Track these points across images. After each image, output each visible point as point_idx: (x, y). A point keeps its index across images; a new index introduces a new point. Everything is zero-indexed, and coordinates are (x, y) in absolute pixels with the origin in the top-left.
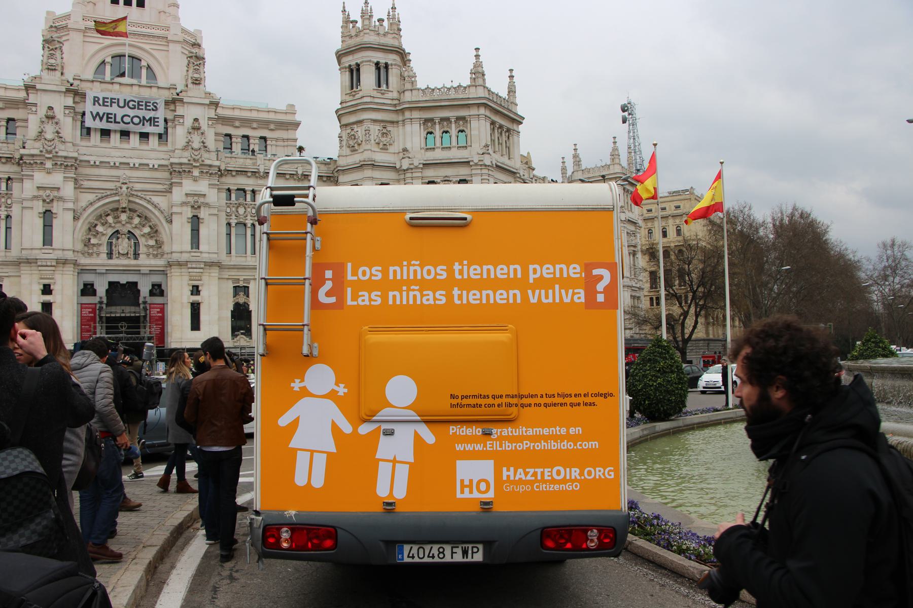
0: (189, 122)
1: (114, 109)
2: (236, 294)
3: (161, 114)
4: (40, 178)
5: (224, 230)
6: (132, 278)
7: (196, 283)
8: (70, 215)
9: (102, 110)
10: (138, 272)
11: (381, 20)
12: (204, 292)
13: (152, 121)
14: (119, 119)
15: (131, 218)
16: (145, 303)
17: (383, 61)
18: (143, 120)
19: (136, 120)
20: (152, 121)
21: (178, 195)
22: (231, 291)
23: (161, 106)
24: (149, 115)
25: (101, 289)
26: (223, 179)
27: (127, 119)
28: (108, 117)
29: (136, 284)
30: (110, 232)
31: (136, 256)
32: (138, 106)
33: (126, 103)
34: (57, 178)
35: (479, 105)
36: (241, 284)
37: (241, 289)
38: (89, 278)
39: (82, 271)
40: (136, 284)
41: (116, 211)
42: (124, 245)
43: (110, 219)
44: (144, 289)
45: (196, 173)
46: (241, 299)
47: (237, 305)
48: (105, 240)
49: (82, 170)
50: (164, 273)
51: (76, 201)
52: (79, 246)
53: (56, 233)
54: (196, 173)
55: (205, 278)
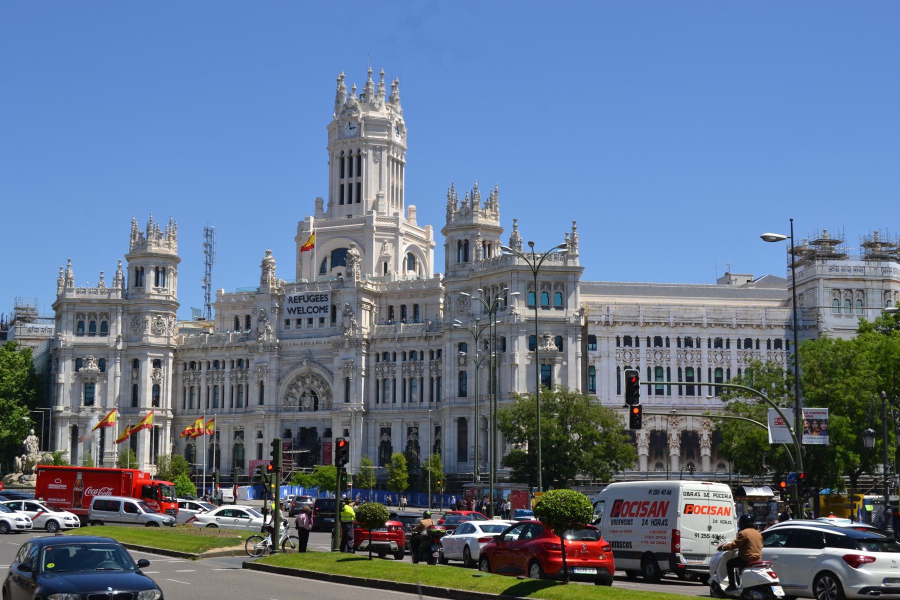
0: (343, 308)
1: (302, 304)
2: (382, 434)
3: (328, 304)
4: (256, 358)
5: (373, 385)
6: (313, 425)
7: (346, 427)
8: (273, 384)
9: (294, 306)
10: (316, 420)
11: (463, 203)
12: (352, 434)
13: (325, 309)
14: (305, 311)
15: (312, 382)
16: (319, 441)
17: (463, 239)
18: (320, 309)
19: (316, 310)
20: (325, 309)
21: (337, 362)
22: (379, 432)
23: (329, 297)
24: (322, 304)
25: (295, 434)
26: (372, 347)
27: (310, 310)
28: (299, 310)
29: (315, 428)
30: (301, 390)
31: (316, 409)
32: (316, 300)
33: (309, 298)
34: (267, 357)
35: (512, 271)
36: (385, 426)
37: (386, 431)
38: (288, 426)
39: (283, 421)
40: (315, 428)
41: (302, 378)
42: (308, 402)
43: (300, 383)
44: (320, 433)
45: (347, 346)
46: (385, 438)
47: (383, 442)
48: (298, 396)
49: (283, 350)
50: (331, 420)
51: (279, 371)
52: (281, 403)
53: (265, 396)
54: (347, 346)
55: (353, 424)
